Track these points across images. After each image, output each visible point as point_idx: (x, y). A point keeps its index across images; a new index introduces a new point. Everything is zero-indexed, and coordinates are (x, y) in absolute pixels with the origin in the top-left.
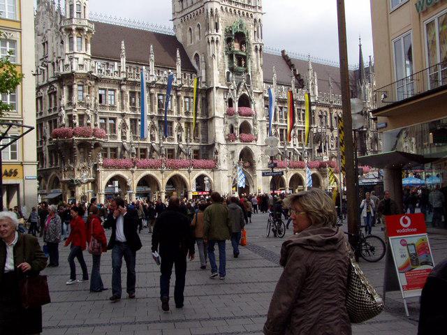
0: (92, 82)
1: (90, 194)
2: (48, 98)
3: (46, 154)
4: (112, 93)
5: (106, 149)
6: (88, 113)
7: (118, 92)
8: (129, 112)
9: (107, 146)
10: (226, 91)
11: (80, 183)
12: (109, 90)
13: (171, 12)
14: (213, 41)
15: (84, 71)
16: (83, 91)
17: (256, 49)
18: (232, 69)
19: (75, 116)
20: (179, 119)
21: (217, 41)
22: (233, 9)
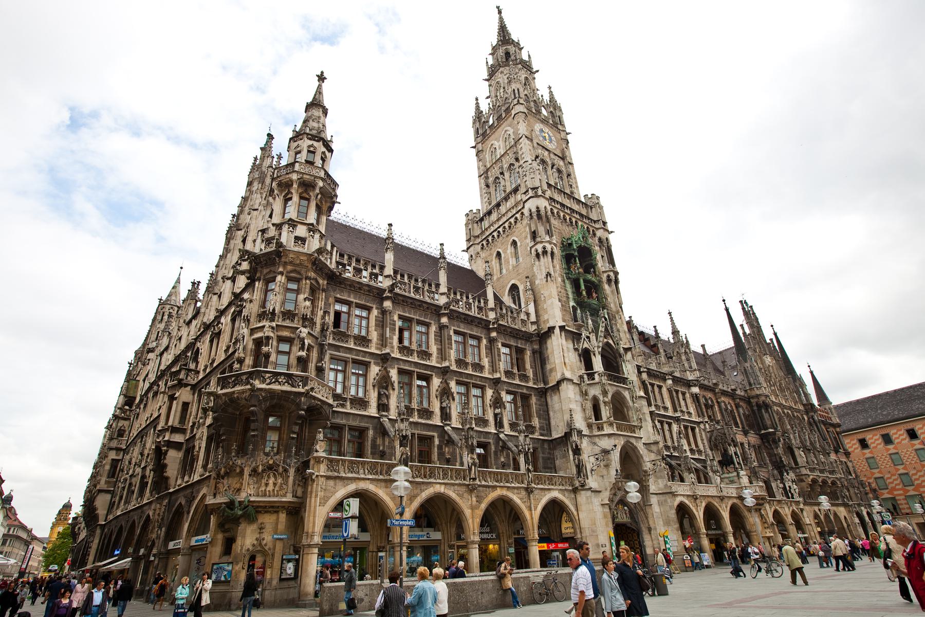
0: (321, 282)
1: (279, 546)
2: (230, 325)
3: (201, 445)
4: (364, 314)
5: (339, 428)
6: (303, 335)
7: (375, 312)
8: (396, 354)
9: (343, 422)
10: (575, 337)
11: (252, 512)
12: (359, 306)
13: (464, 237)
14: (545, 252)
15: (305, 251)
16: (298, 292)
17: (609, 280)
18: (581, 304)
19: (268, 338)
20: (497, 382)
21: (552, 254)
22: (568, 218)
